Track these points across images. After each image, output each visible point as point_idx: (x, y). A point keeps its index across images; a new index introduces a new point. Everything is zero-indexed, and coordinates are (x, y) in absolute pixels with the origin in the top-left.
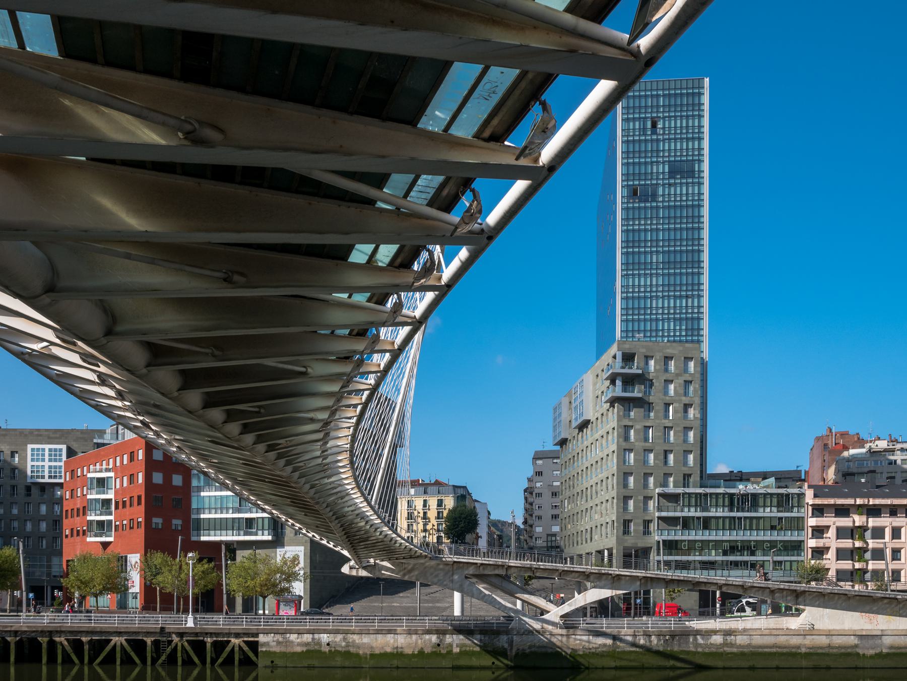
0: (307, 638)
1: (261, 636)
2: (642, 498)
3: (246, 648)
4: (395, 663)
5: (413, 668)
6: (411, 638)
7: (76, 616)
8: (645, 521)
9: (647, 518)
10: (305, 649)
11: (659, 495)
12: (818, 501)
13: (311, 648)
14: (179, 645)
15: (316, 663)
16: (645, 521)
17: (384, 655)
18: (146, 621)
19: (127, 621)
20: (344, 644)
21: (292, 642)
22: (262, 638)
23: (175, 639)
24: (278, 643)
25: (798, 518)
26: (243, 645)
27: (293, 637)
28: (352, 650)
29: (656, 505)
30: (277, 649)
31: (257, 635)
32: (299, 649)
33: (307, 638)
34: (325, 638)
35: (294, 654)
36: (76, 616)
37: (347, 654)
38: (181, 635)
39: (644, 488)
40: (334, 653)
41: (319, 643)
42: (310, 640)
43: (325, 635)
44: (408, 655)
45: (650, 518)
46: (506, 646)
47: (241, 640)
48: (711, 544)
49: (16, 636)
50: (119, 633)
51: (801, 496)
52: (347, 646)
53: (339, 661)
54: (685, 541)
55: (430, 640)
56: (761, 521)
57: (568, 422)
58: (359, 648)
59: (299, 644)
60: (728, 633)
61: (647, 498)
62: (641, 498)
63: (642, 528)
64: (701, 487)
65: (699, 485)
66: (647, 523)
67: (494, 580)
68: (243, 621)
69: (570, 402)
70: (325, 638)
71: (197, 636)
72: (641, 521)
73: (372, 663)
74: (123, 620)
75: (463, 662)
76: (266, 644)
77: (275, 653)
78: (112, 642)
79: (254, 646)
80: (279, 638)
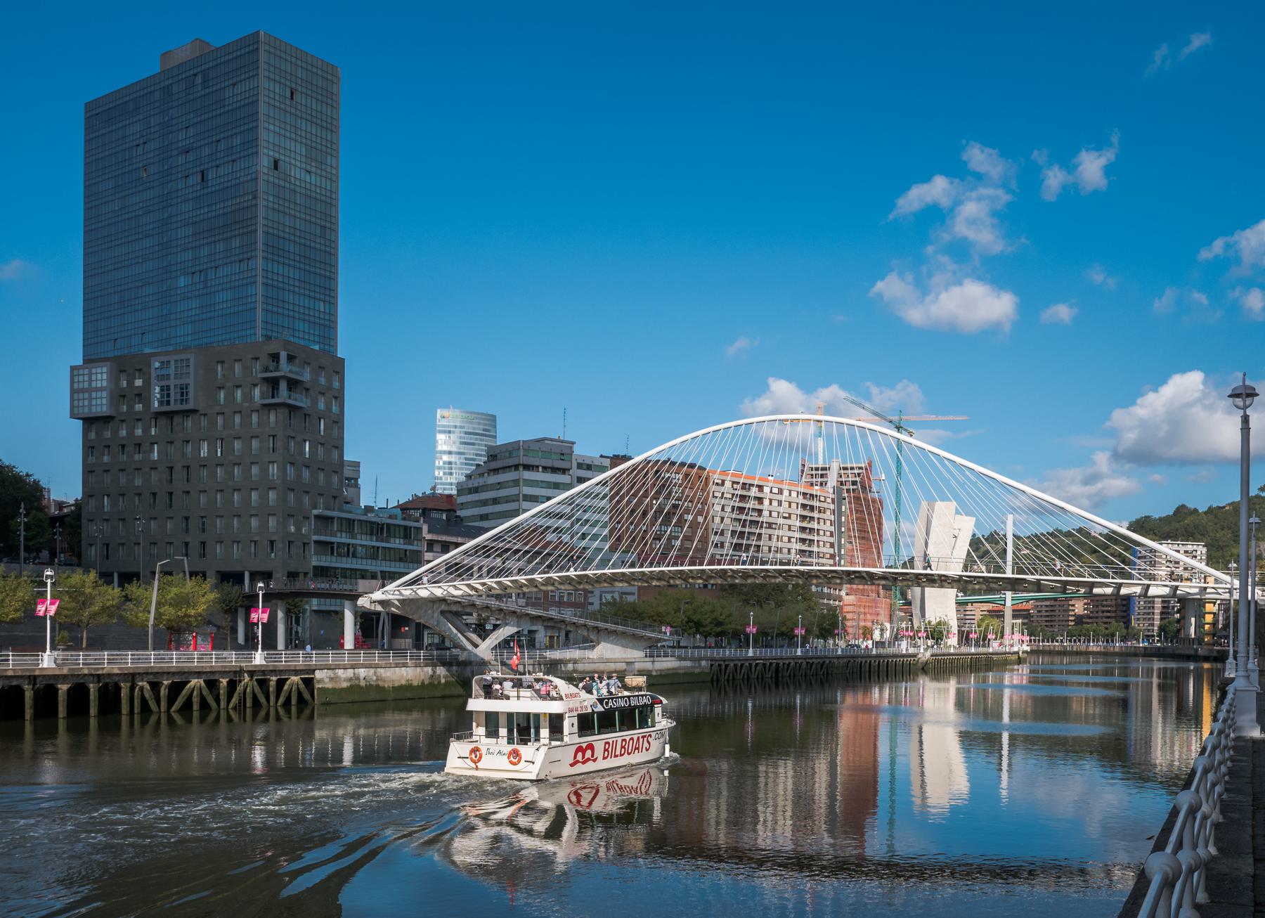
0: (350, 673)
1: (317, 672)
3: (302, 686)
4: (408, 695)
5: (419, 698)
6: (369, 671)
7: (90, 655)
9: (305, 541)
10: (349, 684)
12: (435, 537)
13: (353, 683)
14: (250, 684)
15: (356, 698)
17: (401, 688)
18: (161, 659)
19: (143, 659)
20: (375, 678)
21: (340, 678)
22: (319, 675)
23: (247, 678)
24: (331, 679)
25: (417, 551)
26: (300, 682)
27: (340, 672)
28: (381, 684)
30: (329, 686)
31: (313, 671)
32: (345, 685)
33: (350, 673)
34: (362, 672)
35: (342, 689)
36: (90, 655)
37: (378, 688)
38: (252, 673)
40: (369, 687)
41: (358, 679)
42: (352, 675)
43: (362, 670)
44: (415, 686)
46: (470, 675)
47: (298, 677)
48: (358, 573)
49: (99, 682)
50: (198, 674)
51: (419, 530)
52: (377, 680)
53: (372, 696)
54: (338, 568)
55: (428, 672)
56: (392, 552)
58: (385, 681)
59: (346, 680)
60: (575, 662)
67: (450, 616)
68: (212, 658)
70: (362, 672)
71: (265, 675)
73: (392, 696)
74: (139, 659)
75: (447, 692)
76: (320, 681)
77: (328, 689)
78: (288, 683)
79: (309, 683)
80: (330, 673)
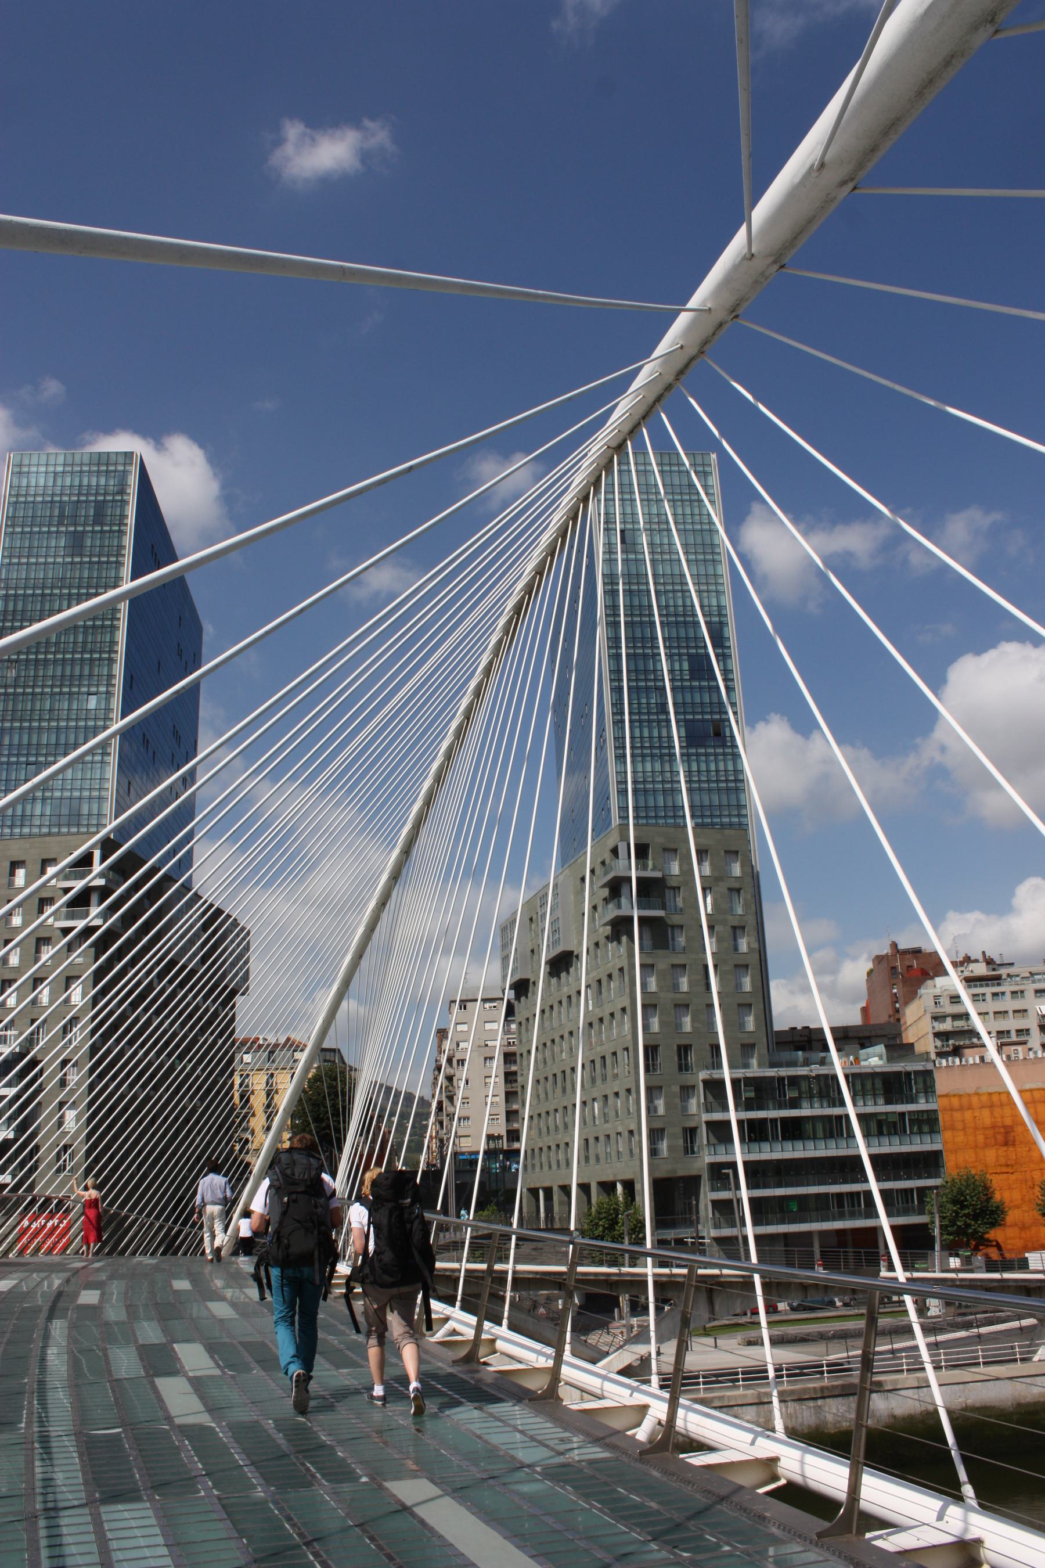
2: (678, 1090)
8: (685, 1130)
11: (705, 1082)
16: (685, 1130)
29: (702, 1100)
39: (680, 1069)
45: (692, 1124)
57: (529, 953)
61: (687, 1090)
62: (676, 1089)
63: (681, 1142)
64: (772, 1065)
65: (767, 1064)
66: (691, 1133)
69: (531, 919)
72: (678, 1131)
